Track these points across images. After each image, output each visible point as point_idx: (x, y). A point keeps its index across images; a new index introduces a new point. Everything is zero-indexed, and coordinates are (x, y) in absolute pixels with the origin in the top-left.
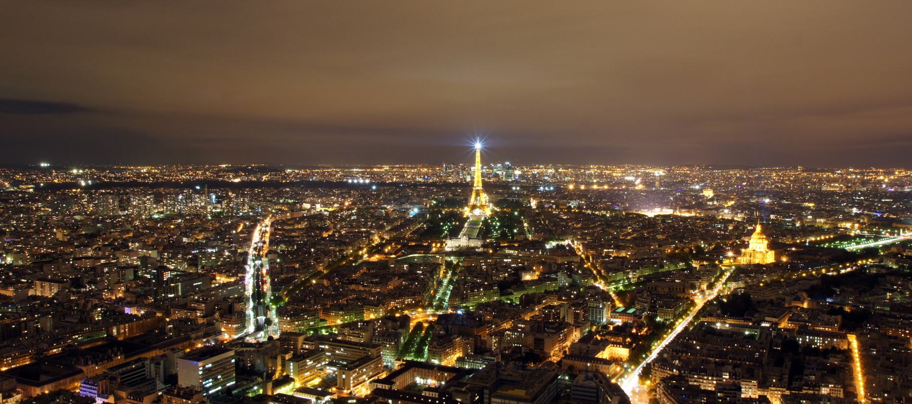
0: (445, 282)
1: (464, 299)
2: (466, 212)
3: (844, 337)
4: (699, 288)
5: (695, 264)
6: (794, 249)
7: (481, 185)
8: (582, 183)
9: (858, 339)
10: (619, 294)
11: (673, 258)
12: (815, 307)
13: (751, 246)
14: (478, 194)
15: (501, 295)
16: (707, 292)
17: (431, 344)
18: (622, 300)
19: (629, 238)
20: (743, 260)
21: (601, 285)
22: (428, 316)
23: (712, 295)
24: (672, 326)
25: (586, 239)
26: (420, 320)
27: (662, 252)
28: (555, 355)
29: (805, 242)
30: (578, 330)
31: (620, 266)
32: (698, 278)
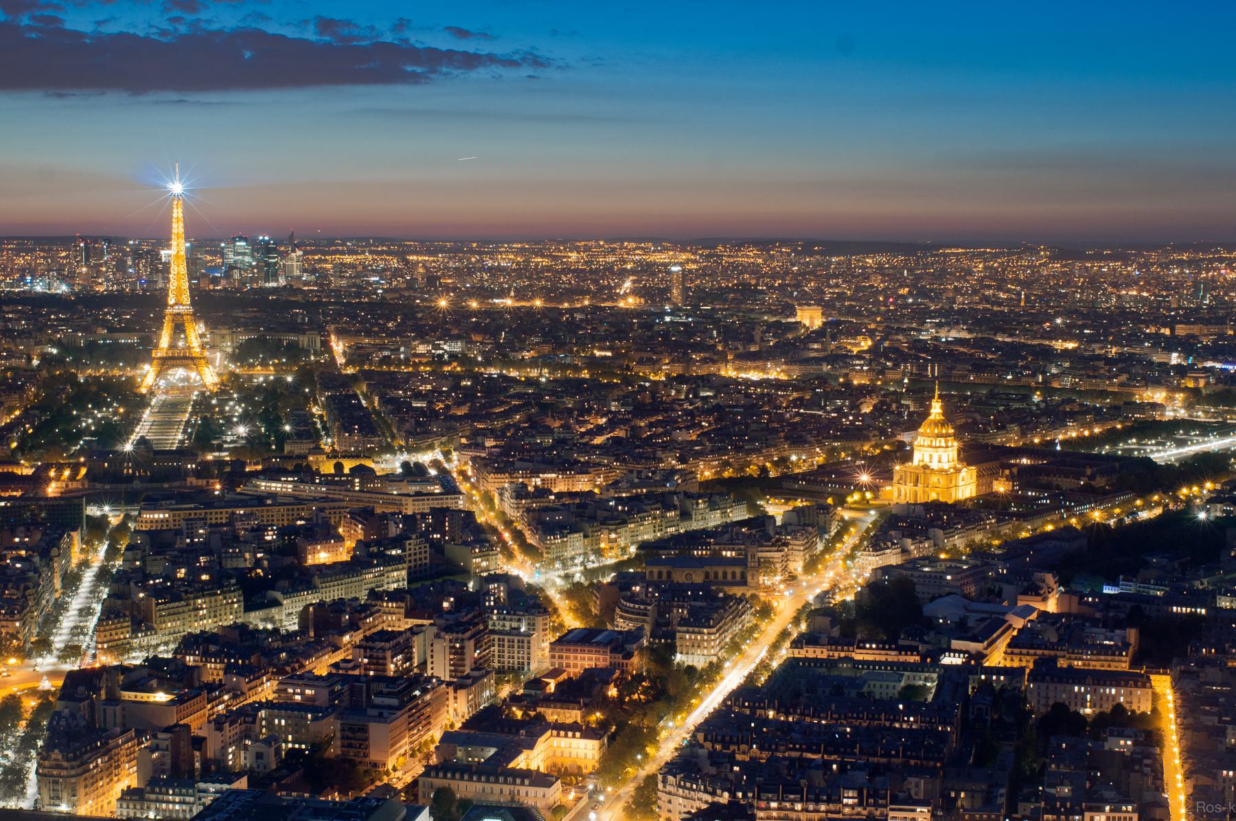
0: (88, 577)
1: (142, 623)
2: (147, 376)
3: (1144, 682)
4: (785, 569)
5: (776, 509)
6: (1024, 461)
7: (186, 299)
8: (471, 293)
9: (1176, 686)
10: (574, 592)
11: (716, 492)
12: (1075, 608)
13: (917, 456)
14: (179, 328)
15: (249, 608)
16: (804, 580)
17: (43, 756)
18: (582, 611)
19: (598, 440)
20: (898, 493)
21: (524, 571)
22: (39, 677)
23: (812, 589)
24: (712, 672)
25: (481, 447)
26: (14, 689)
27: (687, 475)
28: (400, 763)
29: (1052, 443)
30: (462, 694)
31: (583, 516)
32: (781, 545)
